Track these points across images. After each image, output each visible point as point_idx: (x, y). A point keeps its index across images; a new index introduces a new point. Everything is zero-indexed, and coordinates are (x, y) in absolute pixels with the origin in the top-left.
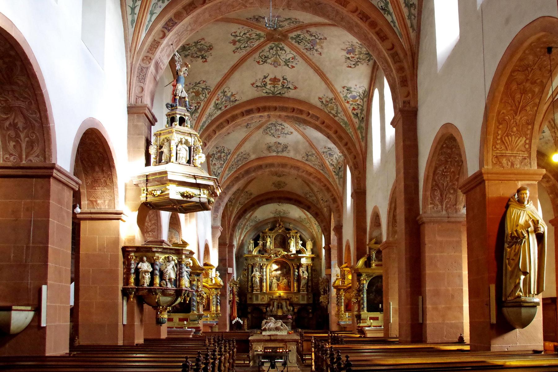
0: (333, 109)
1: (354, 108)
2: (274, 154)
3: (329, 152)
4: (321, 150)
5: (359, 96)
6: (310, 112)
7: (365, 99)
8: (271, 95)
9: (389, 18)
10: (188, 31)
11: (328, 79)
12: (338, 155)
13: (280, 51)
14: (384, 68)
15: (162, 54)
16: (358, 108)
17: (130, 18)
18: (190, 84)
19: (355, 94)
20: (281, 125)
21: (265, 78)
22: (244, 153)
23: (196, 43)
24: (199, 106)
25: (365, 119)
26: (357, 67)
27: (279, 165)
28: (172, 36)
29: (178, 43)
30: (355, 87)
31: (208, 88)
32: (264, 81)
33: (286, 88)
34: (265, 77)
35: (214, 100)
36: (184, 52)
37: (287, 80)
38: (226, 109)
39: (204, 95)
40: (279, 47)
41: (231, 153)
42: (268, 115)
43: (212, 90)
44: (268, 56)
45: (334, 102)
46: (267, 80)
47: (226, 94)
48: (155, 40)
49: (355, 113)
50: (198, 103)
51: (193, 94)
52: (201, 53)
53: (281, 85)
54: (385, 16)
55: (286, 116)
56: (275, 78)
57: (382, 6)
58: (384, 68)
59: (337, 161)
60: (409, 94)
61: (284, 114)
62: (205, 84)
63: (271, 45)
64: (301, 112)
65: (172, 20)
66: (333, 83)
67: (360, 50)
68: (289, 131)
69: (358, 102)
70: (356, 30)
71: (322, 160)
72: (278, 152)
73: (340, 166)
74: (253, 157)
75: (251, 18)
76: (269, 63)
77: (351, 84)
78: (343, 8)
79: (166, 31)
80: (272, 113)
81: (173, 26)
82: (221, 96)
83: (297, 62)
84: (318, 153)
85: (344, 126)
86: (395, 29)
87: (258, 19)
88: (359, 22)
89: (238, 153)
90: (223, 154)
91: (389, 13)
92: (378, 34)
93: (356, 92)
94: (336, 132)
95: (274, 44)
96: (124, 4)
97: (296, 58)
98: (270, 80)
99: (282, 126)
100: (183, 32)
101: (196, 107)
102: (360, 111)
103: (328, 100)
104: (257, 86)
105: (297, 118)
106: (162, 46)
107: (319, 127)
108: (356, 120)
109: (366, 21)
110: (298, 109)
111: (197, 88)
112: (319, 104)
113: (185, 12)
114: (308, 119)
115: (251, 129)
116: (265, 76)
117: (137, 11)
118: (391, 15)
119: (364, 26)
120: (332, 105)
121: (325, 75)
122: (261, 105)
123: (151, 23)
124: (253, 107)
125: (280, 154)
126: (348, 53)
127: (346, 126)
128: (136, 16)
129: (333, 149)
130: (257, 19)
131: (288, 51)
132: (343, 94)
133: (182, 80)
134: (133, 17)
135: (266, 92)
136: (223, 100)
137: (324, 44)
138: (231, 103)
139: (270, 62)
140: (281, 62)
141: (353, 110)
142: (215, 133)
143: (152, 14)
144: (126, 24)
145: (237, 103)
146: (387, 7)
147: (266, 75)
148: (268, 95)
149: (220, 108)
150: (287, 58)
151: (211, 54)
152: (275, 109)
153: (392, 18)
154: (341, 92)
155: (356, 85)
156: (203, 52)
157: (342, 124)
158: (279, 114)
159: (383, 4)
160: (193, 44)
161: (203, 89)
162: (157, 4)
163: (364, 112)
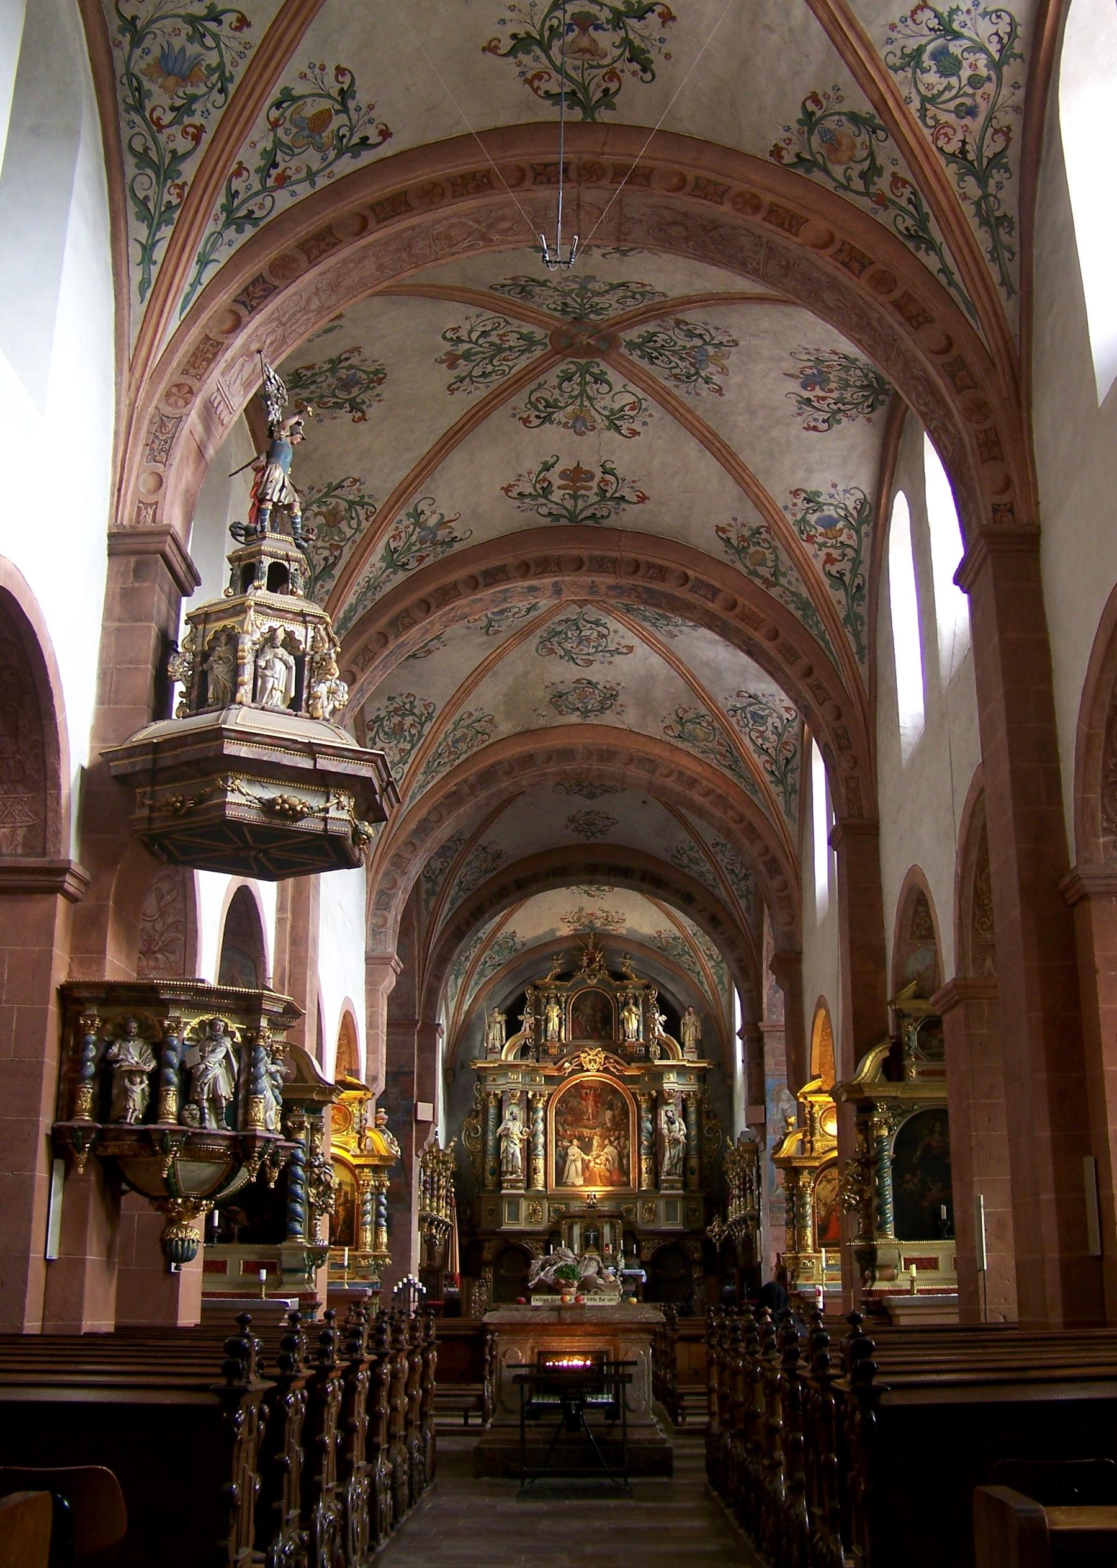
0: (762, 562)
1: (829, 555)
2: (574, 718)
3: (751, 709)
4: (725, 701)
5: (846, 517)
6: (690, 572)
7: (865, 528)
8: (563, 522)
9: (931, 262)
10: (308, 312)
11: (744, 469)
12: (780, 717)
13: (595, 387)
14: (923, 409)
15: (227, 378)
16: (845, 555)
17: (136, 274)
18: (311, 488)
19: (835, 515)
20: (597, 623)
21: (548, 470)
22: (477, 715)
23: (335, 363)
24: (337, 559)
25: (866, 591)
26: (836, 427)
27: (589, 754)
28: (261, 325)
29: (276, 349)
30: (833, 491)
31: (366, 500)
32: (544, 480)
33: (612, 498)
34: (547, 467)
35: (385, 539)
36: (297, 390)
37: (614, 475)
38: (422, 566)
39: (354, 523)
40: (592, 374)
41: (436, 715)
42: (555, 584)
43: (379, 506)
44: (556, 400)
45: (765, 540)
46: (554, 476)
47: (422, 518)
48: (207, 337)
49: (834, 573)
50: (333, 547)
51: (321, 520)
52: (350, 393)
53: (595, 490)
54: (921, 255)
55: (611, 587)
56: (578, 468)
57: (907, 229)
58: (923, 409)
59: (780, 735)
60: (1008, 483)
61: (605, 580)
62: (359, 490)
63: (562, 366)
64: (661, 573)
65: (264, 281)
66: (760, 478)
67: (843, 376)
68: (624, 642)
69: (843, 538)
70: (830, 298)
71: (729, 735)
72: (585, 713)
73: (789, 755)
74: (506, 728)
75: (503, 286)
76: (559, 423)
77: (819, 482)
78: (787, 235)
79: (243, 311)
80: (567, 578)
81: (265, 297)
82: (407, 527)
83: (647, 419)
84: (716, 714)
85: (798, 614)
86: (952, 291)
87: (524, 288)
88: (843, 276)
89: (457, 717)
90: (409, 720)
91: (931, 246)
92: (898, 306)
93: (836, 507)
94: (774, 635)
95: (572, 362)
96: (123, 233)
97: (644, 404)
99: (600, 629)
100: (294, 314)
101: (326, 559)
102: (850, 564)
103: (747, 533)
105: (649, 591)
106: (229, 355)
107: (719, 618)
108: (837, 596)
109: (861, 272)
110: (650, 566)
111: (334, 501)
112: (717, 549)
113: (305, 258)
114: (683, 593)
115: (502, 637)
116: (545, 463)
117: (159, 254)
118: (939, 253)
119: (859, 287)
120: (760, 549)
121: (734, 456)
122: (531, 553)
123: (200, 289)
124: (508, 559)
125: (592, 720)
126: (804, 386)
127: (805, 616)
128: (155, 270)
129: (764, 700)
130: (523, 289)
131: (618, 388)
132: (794, 515)
133: (288, 456)
134: (147, 272)
135: (550, 514)
136: (414, 538)
137: (731, 361)
138: (439, 549)
139: (563, 420)
140: (598, 418)
141: (825, 563)
142: (386, 642)
143: (203, 263)
144: (125, 290)
145: (457, 547)
146: (925, 229)
148: (556, 524)
149: (404, 564)
150: (617, 406)
151: (378, 395)
152: (578, 564)
153: (942, 261)
154: (786, 508)
155: (834, 486)
156: (355, 391)
157: (791, 607)
158: (589, 579)
159: (910, 222)
160: (327, 366)
161: (351, 504)
162: (220, 234)
163: (864, 569)
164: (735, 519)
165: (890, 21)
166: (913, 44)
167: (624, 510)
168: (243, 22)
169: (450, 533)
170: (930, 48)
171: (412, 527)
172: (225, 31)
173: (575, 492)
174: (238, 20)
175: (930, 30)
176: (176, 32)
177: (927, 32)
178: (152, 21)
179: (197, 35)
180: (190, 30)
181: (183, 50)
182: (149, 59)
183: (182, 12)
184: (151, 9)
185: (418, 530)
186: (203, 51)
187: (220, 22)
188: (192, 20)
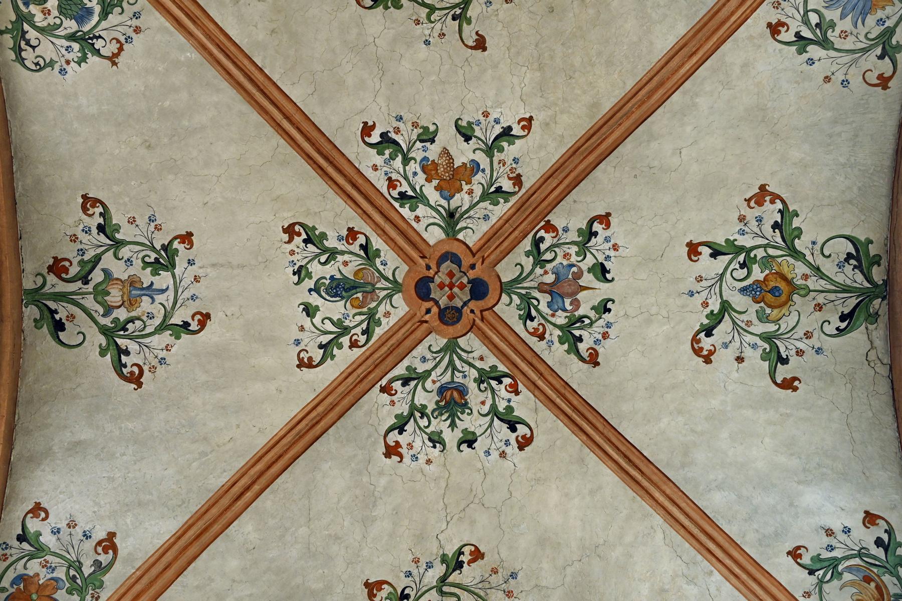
165: (141, 35)
166: (113, 19)
168: (775, 29)
170: (96, 18)
172: (795, 25)
174: (779, 32)
175: (100, 37)
176: (844, 35)
177: (103, 34)
178: (865, 50)
179: (824, 27)
180: (829, 33)
181: (843, 16)
182: (880, 14)
183: (833, 53)
184: (862, 61)
186: (823, 10)
187: (798, 35)
188: (824, 43)
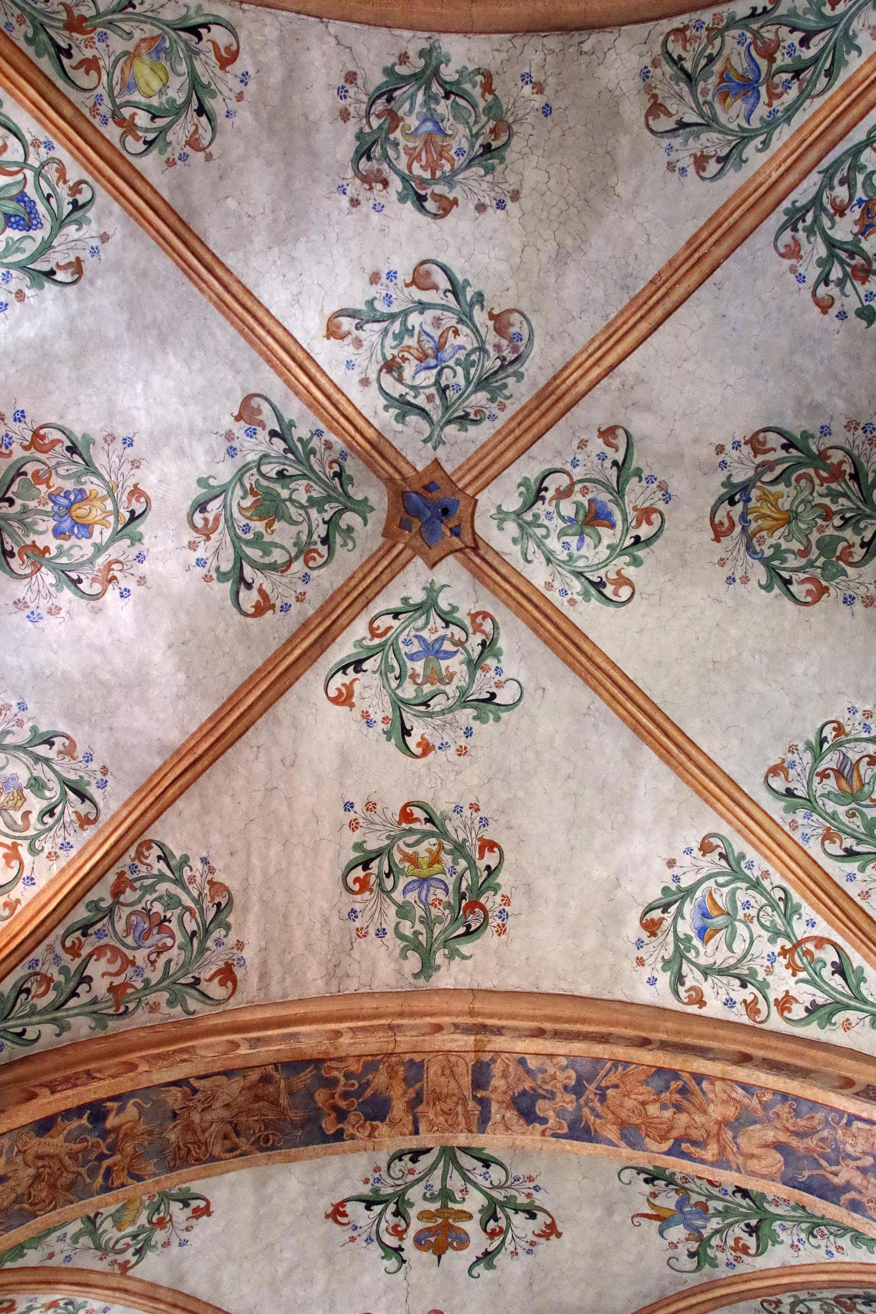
21: (486, 1254)
32: (492, 1235)
34: (487, 1258)
46: (478, 1242)
47: (694, 1246)
53: (413, 1213)
98: (463, 1242)
103: (159, 1236)
104: (533, 1216)
116: (490, 1266)
136: (715, 1223)
147: (479, 1269)
164: (183, 1243)
167: (366, 1181)
169: (654, 1195)
171: (713, 1242)
173: (444, 1206)
185: (706, 1233)
